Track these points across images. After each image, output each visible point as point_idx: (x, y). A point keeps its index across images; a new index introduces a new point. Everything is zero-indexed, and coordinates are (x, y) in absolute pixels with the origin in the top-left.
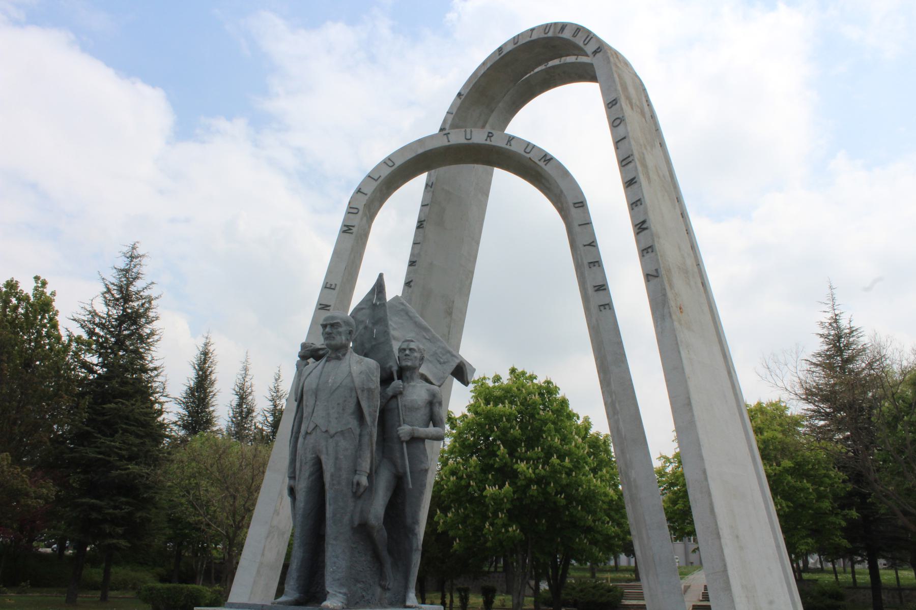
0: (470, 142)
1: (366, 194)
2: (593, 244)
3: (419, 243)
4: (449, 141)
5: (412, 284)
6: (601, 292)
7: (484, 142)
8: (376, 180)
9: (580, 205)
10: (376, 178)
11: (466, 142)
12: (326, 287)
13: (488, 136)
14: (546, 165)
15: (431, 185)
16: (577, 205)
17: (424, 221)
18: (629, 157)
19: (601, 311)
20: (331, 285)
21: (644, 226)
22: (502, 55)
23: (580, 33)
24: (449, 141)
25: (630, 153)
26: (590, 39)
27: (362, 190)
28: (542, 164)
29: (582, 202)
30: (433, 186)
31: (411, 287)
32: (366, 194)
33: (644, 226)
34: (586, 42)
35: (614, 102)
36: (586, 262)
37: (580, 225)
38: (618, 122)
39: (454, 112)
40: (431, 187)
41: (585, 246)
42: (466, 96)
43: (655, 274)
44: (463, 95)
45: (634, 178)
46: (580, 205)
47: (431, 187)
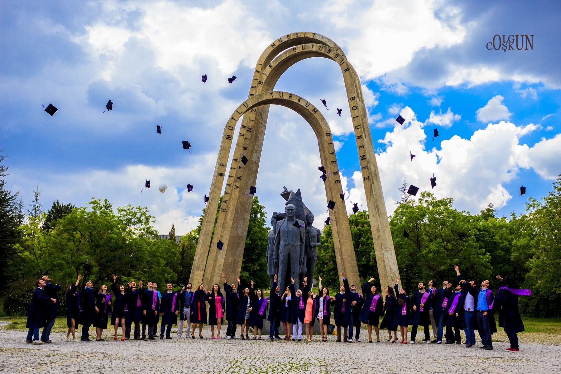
0: (282, 98)
4: (272, 97)
6: (336, 175)
7: (288, 99)
10: (240, 112)
11: (280, 98)
12: (221, 165)
13: (290, 96)
14: (315, 113)
16: (327, 134)
20: (223, 164)
21: (364, 158)
22: (296, 52)
24: (272, 97)
28: (313, 113)
29: (330, 133)
33: (364, 158)
35: (354, 98)
39: (267, 75)
40: (255, 112)
42: (274, 68)
43: (368, 178)
45: (361, 136)
46: (329, 134)
47: (255, 112)
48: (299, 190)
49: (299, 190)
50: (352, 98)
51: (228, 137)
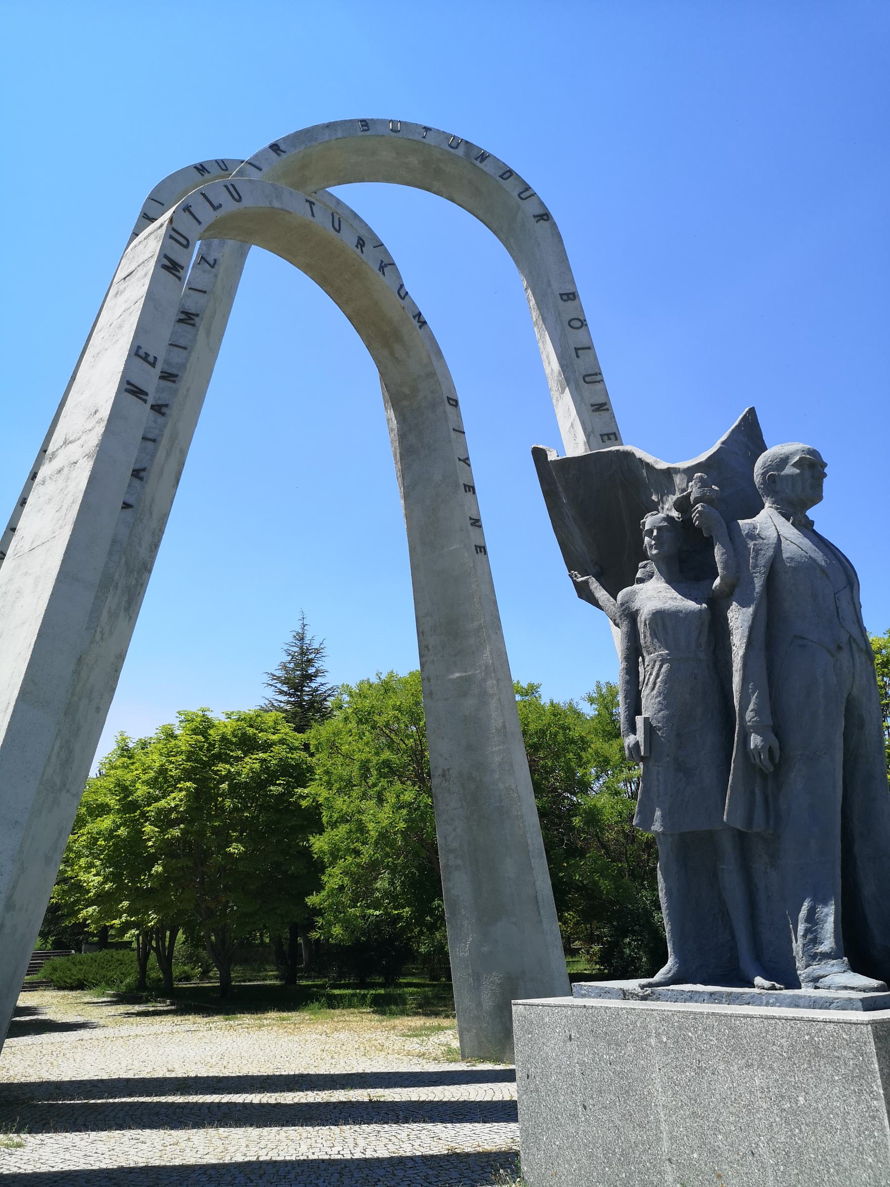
1: (200, 223)
2: (467, 461)
3: (185, 348)
5: (164, 410)
8: (215, 208)
9: (454, 403)
15: (212, 262)
17: (197, 315)
18: (596, 374)
19: (477, 553)
23: (511, 178)
25: (597, 371)
26: (530, 196)
27: (191, 209)
30: (216, 266)
31: (163, 414)
32: (200, 223)
34: (523, 196)
36: (461, 483)
37: (454, 429)
38: (578, 324)
41: (460, 459)
44: (284, 152)
47: (212, 267)
48: (752, 411)
49: (752, 411)
50: (567, 294)
51: (168, 264)
